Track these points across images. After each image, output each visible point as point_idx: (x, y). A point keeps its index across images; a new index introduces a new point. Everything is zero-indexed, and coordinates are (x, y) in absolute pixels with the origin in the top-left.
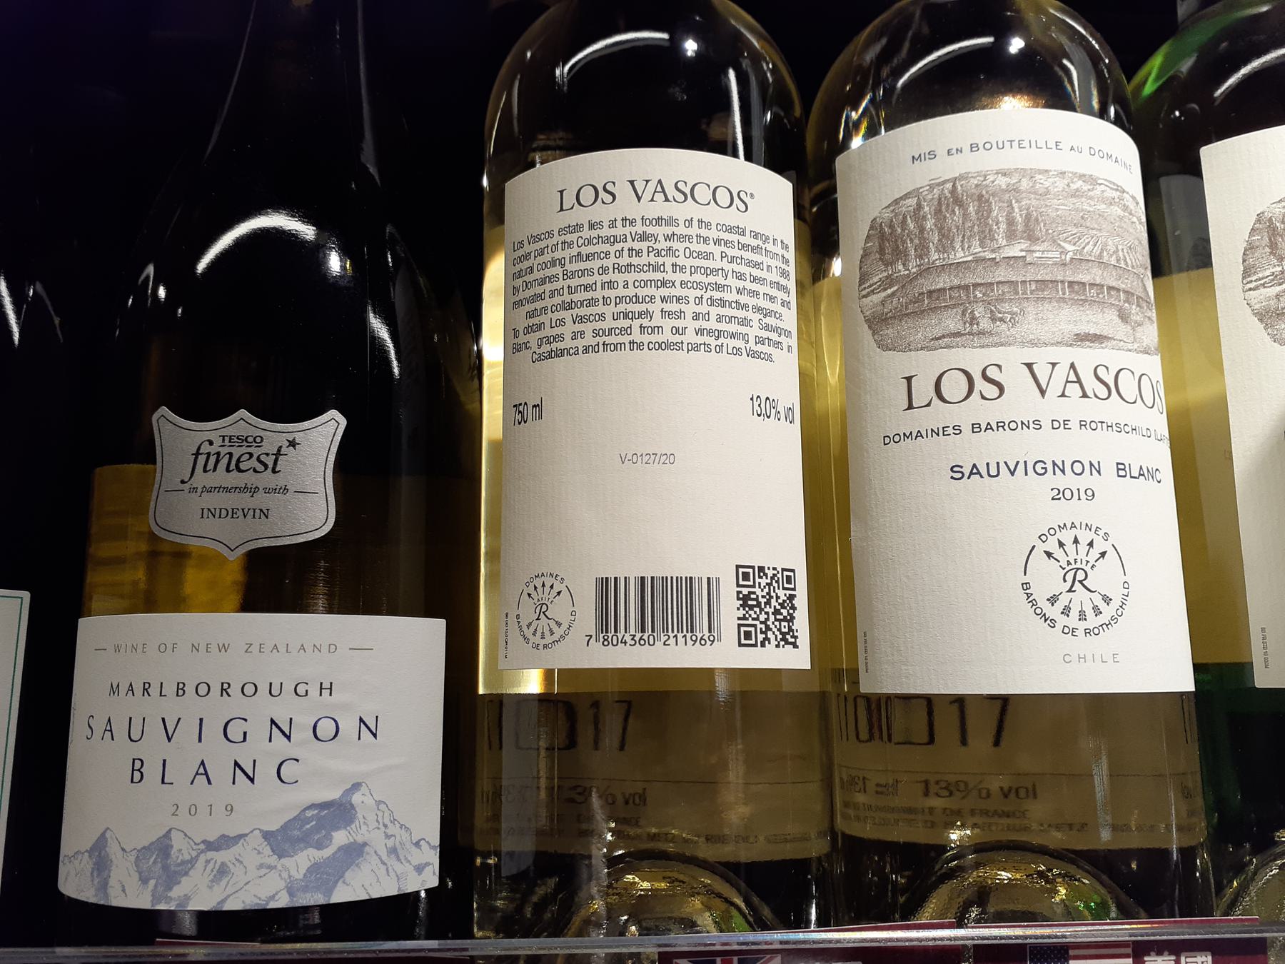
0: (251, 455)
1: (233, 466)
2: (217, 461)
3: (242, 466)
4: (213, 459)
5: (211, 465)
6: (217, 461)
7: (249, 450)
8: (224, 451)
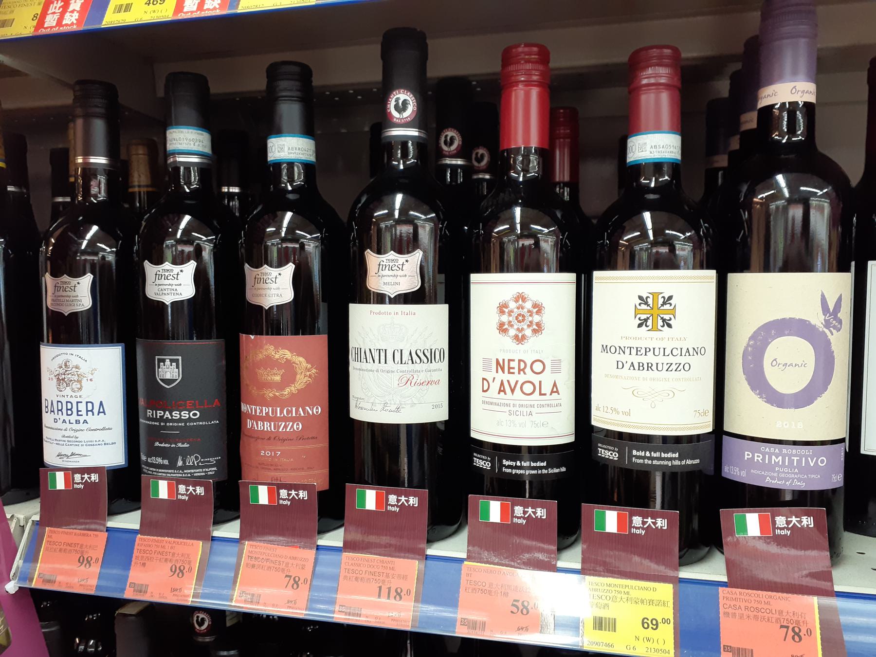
0: (395, 265)
1: (390, 269)
2: (386, 267)
3: (393, 269)
4: (384, 267)
5: (384, 269)
6: (386, 267)
7: (395, 264)
8: (387, 264)
